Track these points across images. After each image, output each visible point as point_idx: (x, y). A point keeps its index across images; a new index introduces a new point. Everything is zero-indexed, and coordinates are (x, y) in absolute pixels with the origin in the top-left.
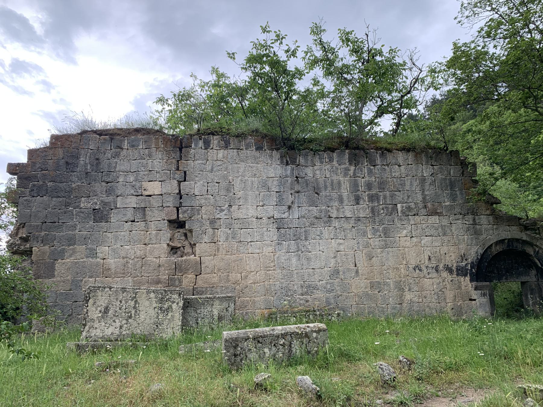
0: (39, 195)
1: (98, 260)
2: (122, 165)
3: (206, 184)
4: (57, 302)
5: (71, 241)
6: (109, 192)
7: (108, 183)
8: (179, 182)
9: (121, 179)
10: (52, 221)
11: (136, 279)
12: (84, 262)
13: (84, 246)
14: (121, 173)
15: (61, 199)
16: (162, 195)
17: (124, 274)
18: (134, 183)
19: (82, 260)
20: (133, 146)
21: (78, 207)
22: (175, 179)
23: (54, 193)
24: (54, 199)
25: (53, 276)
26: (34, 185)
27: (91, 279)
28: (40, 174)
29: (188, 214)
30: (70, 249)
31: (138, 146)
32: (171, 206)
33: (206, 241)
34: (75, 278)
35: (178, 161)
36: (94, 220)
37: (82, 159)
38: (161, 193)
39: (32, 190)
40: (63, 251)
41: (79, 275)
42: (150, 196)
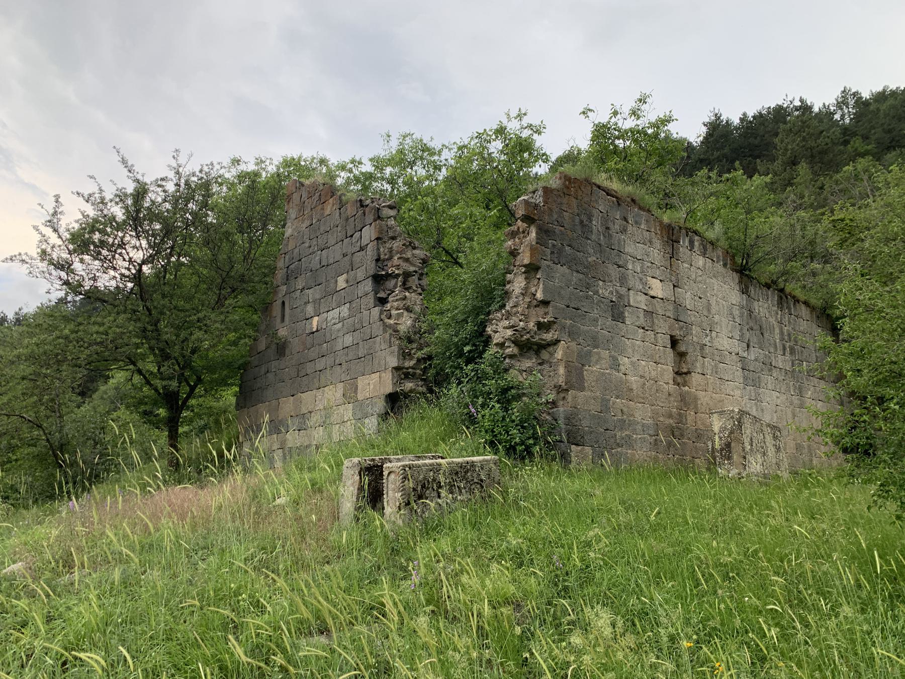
2: (630, 248)
4: (591, 428)
6: (623, 280)
7: (619, 267)
11: (653, 408)
12: (609, 374)
15: (581, 276)
16: (662, 299)
18: (640, 275)
19: (608, 371)
20: (636, 223)
21: (596, 293)
23: (573, 264)
24: (575, 274)
25: (582, 389)
26: (554, 245)
28: (558, 229)
31: (640, 224)
35: (671, 258)
36: (613, 316)
37: (594, 223)
39: (552, 253)
40: (589, 353)
42: (653, 297)
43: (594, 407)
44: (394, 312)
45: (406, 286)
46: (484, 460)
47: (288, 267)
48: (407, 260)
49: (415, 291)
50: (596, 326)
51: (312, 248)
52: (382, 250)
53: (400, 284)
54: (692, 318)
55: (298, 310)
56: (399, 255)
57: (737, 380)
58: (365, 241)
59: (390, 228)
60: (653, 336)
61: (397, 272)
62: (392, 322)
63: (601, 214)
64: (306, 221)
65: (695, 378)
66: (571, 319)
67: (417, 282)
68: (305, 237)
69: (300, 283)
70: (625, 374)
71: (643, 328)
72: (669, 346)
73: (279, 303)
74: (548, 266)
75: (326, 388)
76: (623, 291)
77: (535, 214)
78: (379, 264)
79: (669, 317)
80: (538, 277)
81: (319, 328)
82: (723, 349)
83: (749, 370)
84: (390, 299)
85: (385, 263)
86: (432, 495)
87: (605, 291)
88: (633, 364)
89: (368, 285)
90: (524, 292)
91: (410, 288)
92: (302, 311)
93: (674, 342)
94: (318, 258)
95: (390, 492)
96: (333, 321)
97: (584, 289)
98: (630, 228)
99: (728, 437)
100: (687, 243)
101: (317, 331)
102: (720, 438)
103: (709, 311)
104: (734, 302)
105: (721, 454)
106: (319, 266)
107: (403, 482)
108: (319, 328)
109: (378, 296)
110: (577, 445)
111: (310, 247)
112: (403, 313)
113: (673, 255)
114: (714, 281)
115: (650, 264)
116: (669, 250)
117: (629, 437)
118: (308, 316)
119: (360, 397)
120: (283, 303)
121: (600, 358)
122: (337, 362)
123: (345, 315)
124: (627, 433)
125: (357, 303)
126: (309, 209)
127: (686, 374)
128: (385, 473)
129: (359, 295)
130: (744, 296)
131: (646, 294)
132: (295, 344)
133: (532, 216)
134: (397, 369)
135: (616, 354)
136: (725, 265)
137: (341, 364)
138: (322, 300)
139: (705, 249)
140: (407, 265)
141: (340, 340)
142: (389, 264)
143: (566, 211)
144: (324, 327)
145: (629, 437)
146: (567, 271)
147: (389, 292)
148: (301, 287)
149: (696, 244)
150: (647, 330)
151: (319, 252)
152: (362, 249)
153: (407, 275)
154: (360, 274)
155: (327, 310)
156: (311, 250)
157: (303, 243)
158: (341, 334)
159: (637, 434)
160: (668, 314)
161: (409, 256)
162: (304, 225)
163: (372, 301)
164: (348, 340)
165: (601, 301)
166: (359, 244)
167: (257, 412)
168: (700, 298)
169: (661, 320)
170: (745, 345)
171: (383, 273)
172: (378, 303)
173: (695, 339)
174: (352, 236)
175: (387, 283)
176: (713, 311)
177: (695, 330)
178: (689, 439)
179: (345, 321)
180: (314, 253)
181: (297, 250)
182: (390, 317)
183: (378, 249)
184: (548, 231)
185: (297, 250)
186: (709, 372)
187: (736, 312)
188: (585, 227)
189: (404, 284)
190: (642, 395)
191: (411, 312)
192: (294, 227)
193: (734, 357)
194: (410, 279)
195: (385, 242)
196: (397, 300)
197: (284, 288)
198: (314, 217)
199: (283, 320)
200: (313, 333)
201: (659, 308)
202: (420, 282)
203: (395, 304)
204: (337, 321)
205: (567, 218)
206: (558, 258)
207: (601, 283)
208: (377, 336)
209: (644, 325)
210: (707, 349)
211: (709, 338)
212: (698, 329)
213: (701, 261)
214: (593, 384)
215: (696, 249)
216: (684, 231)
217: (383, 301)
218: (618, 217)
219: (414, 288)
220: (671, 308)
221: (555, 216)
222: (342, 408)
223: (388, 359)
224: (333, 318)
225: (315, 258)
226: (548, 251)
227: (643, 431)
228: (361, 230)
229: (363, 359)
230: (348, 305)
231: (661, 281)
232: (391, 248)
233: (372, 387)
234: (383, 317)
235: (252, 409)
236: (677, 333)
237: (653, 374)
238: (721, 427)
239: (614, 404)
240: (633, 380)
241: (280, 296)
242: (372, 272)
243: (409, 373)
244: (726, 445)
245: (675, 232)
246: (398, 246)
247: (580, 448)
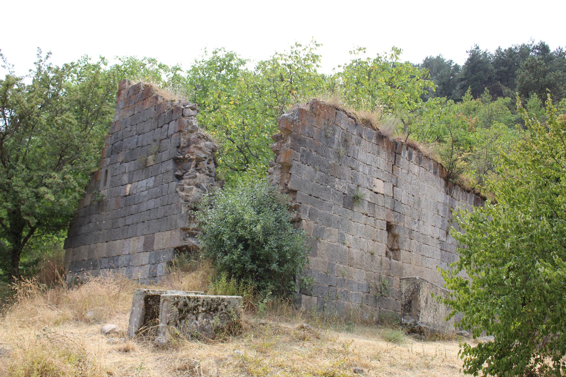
0: (307, 163)
1: (345, 247)
2: (362, 156)
3: (407, 194)
4: (319, 283)
5: (328, 221)
8: (394, 186)
9: (361, 169)
10: (316, 196)
11: (367, 272)
12: (337, 246)
13: (337, 230)
14: (361, 163)
15: (323, 174)
16: (383, 195)
17: (361, 265)
18: (368, 176)
19: (335, 244)
20: (369, 138)
21: (333, 186)
22: (392, 182)
24: (318, 172)
25: (315, 255)
26: (304, 151)
27: (341, 265)
28: (308, 139)
29: (397, 219)
30: (328, 230)
31: (371, 139)
32: (389, 208)
33: (406, 249)
34: (330, 261)
35: (393, 165)
36: (344, 204)
38: (383, 193)
39: (302, 156)
40: (322, 230)
41: (334, 258)
42: (376, 193)
43: (322, 269)
44: (186, 187)
45: (198, 168)
46: (231, 298)
47: (113, 145)
48: (200, 149)
49: (203, 172)
50: (330, 210)
51: (132, 132)
52: (182, 139)
53: (193, 166)
54: (404, 209)
55: (117, 177)
56: (194, 145)
57: (435, 257)
58: (171, 132)
59: (190, 124)
60: (373, 221)
61: (191, 157)
62: (183, 194)
63: (342, 130)
64: (130, 111)
65: (403, 254)
66: (311, 204)
67: (206, 165)
68: (128, 123)
69: (121, 158)
70: (349, 247)
71: (366, 215)
72: (385, 229)
73: (103, 171)
74: (298, 165)
75: (132, 239)
76: (353, 186)
77: (291, 128)
78: (179, 150)
79: (387, 208)
80: (290, 172)
81: (131, 193)
82: (426, 234)
83: (446, 251)
84: (185, 177)
85: (184, 150)
86: (192, 318)
87: (341, 186)
88: (355, 240)
89: (170, 165)
90: (279, 182)
91: (200, 169)
92: (120, 179)
93: (389, 227)
94: (135, 140)
95: (163, 313)
96: (142, 189)
97: (324, 183)
98: (363, 142)
99: (411, 296)
100: (407, 155)
101: (129, 195)
102: (405, 297)
103: (419, 205)
104: (440, 201)
105: (405, 308)
106: (135, 146)
107: (172, 307)
108: (131, 193)
109: (176, 173)
110: (307, 295)
111: (131, 131)
112: (192, 188)
113: (395, 163)
114: (425, 184)
115: (376, 169)
116: (392, 159)
117: (347, 292)
118: (124, 183)
119: (155, 247)
120: (107, 171)
121: (331, 234)
122: (141, 220)
123: (151, 185)
124: (346, 289)
125: (160, 177)
126: (133, 103)
127: (397, 250)
128: (162, 300)
129: (163, 172)
130: (448, 197)
131: (371, 190)
132: (112, 203)
133: (289, 129)
134: (184, 229)
135: (343, 232)
136: (435, 173)
137: (144, 222)
138: (135, 172)
139: (420, 160)
140: (200, 152)
141: (145, 204)
142: (187, 150)
143: (316, 127)
144: (134, 193)
145: (347, 292)
146: (312, 169)
147: (184, 171)
148: (120, 160)
149: (414, 156)
150: (369, 216)
151: (137, 136)
152: (168, 137)
153: (199, 160)
154: (165, 156)
155: (137, 180)
156: (131, 134)
157: (126, 128)
158: (146, 199)
159: (353, 291)
160: (386, 206)
161: (202, 146)
162: (128, 115)
163: (171, 177)
164: (151, 204)
165: (336, 193)
166: (166, 133)
167: (80, 251)
168: (413, 196)
169: (381, 210)
170: (444, 232)
171: (181, 157)
172: (175, 178)
173: (406, 225)
174: (162, 127)
175: (184, 164)
176: (422, 206)
177: (407, 219)
178: (393, 297)
179: (150, 190)
180: (133, 136)
181: (120, 133)
182: (183, 190)
183: (180, 139)
184: (301, 140)
185: (120, 133)
186: (414, 250)
187: (441, 208)
188: (328, 139)
189: (196, 166)
190: (360, 263)
191: (199, 187)
192: (121, 115)
193: (435, 240)
194: (201, 163)
195: (185, 134)
196: (189, 178)
197: (108, 160)
198: (136, 109)
199: (105, 184)
200: (126, 196)
201: (380, 200)
202: (209, 166)
203: (187, 181)
204: (144, 189)
205: (315, 132)
206: (306, 160)
207: (337, 180)
208: (172, 204)
209: (368, 212)
210: (414, 234)
211: (417, 225)
212: (410, 219)
213: (416, 169)
214: (323, 252)
215: (413, 160)
216: (404, 147)
217: (179, 178)
218: (355, 133)
219: (204, 170)
220: (389, 201)
221: (307, 130)
222: (142, 254)
223: (178, 221)
224: (142, 187)
225: (133, 140)
226: (299, 154)
227: (358, 288)
228: (169, 124)
229: (160, 220)
230: (153, 178)
231: (384, 181)
232: (189, 139)
233: (165, 241)
234: (178, 189)
235: (76, 249)
236: (393, 220)
237: (371, 248)
238: (406, 289)
239: (338, 267)
240: (355, 252)
241: (105, 165)
242: (173, 156)
243: (192, 233)
244: (408, 302)
245: (398, 146)
246: (194, 138)
247: (308, 297)
